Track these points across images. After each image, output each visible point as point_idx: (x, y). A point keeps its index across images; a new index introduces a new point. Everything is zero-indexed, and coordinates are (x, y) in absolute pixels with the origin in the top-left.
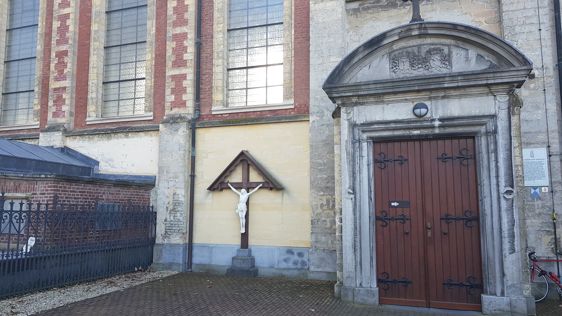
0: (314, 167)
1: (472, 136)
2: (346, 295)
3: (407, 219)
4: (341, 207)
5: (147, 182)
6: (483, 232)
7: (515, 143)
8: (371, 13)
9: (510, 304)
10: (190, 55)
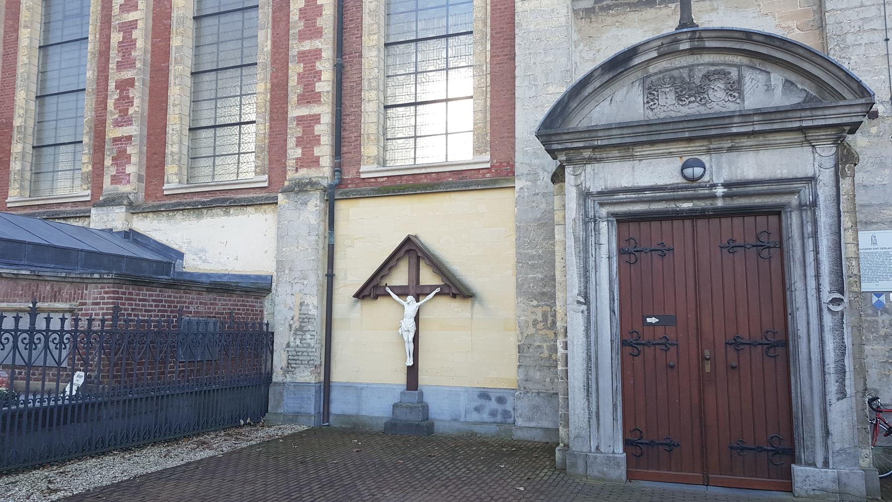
0: (522, 261)
1: (777, 212)
2: (574, 465)
3: (672, 345)
4: (565, 325)
5: (259, 285)
6: (795, 365)
7: (846, 222)
8: (613, 15)
9: (838, 480)
10: (325, 85)
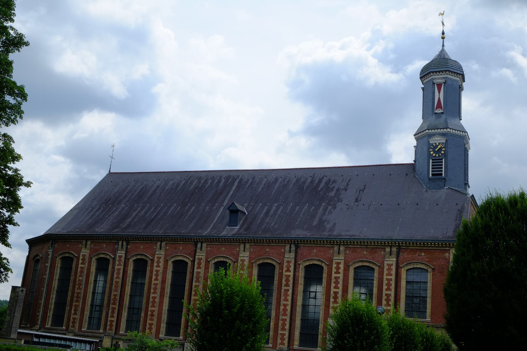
10: (287, 327)
